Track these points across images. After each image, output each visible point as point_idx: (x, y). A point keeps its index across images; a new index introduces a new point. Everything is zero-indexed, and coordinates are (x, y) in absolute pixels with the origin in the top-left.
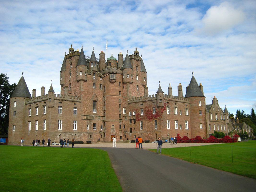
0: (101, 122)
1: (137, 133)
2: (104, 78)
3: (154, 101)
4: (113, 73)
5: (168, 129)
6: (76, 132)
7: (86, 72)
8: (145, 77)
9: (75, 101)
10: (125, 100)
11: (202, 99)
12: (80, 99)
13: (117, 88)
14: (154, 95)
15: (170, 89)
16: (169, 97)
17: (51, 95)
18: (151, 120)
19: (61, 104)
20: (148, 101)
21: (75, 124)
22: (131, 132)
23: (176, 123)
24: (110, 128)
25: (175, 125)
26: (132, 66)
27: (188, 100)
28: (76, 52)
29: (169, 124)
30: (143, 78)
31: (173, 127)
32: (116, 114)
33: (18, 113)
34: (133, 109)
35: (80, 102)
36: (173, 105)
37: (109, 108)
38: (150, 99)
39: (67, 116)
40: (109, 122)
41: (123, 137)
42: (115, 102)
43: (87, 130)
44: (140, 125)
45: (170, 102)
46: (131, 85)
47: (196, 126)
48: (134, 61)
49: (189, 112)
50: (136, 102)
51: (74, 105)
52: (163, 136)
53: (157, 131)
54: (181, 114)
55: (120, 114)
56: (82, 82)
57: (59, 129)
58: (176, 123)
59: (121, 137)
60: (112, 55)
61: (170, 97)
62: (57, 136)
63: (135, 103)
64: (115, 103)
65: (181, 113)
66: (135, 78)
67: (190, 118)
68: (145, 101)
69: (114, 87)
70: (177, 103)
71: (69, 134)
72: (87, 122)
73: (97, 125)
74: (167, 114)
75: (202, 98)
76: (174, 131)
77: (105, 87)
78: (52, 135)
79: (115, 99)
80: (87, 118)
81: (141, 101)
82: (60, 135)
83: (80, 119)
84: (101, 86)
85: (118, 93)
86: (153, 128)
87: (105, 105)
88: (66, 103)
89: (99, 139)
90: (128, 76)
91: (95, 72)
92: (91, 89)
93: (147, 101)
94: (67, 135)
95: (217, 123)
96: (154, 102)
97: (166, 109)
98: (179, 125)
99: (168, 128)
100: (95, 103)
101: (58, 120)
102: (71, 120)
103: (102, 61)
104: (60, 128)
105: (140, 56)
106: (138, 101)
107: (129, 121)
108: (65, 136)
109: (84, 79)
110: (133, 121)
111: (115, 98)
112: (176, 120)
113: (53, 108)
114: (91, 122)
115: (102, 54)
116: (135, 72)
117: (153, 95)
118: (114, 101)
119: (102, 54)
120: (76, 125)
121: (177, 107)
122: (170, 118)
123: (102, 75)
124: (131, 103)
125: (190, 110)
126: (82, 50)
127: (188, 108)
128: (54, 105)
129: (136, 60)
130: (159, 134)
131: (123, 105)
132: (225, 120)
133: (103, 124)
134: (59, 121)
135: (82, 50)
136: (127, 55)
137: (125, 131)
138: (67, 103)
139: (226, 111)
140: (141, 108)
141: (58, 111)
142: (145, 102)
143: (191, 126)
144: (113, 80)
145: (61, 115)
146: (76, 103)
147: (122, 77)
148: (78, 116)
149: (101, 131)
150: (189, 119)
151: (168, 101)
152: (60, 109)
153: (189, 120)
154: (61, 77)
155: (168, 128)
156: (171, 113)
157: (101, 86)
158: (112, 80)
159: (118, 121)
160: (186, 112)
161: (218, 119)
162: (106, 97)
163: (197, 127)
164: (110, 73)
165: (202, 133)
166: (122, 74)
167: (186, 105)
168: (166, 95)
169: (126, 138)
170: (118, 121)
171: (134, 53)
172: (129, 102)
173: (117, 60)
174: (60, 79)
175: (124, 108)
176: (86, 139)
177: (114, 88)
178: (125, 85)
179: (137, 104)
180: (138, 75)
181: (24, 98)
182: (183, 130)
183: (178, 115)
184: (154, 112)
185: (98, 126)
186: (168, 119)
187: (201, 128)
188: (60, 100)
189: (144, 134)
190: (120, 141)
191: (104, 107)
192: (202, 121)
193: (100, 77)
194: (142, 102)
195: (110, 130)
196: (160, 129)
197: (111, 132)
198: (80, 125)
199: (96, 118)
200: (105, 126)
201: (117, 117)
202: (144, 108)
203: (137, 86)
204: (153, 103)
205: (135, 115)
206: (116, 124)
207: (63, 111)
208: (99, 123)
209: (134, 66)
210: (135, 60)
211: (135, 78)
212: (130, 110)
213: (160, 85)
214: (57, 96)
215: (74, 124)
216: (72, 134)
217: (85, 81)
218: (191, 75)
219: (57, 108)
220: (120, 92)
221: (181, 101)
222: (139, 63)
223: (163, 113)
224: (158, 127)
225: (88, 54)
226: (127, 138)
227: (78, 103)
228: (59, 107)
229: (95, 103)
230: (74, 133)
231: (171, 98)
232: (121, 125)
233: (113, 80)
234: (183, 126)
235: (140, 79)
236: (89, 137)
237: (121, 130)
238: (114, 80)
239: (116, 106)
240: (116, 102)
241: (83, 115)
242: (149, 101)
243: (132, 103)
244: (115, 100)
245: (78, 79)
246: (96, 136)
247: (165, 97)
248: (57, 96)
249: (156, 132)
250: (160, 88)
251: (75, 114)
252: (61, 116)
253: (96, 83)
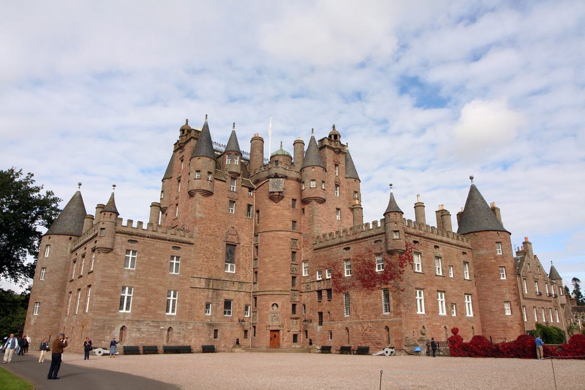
0: (247, 298)
1: (336, 325)
2: (258, 190)
3: (377, 238)
4: (276, 176)
5: (422, 315)
6: (173, 319)
7: (210, 173)
8: (357, 191)
9: (176, 241)
10: (306, 242)
11: (502, 237)
12: (191, 237)
13: (286, 213)
14: (377, 222)
15: (419, 207)
16: (417, 226)
17: (105, 220)
18: (372, 290)
19: (136, 245)
20: (361, 239)
21: (172, 298)
22: (321, 323)
23: (441, 299)
24: (267, 312)
25: (438, 304)
26: (325, 163)
27: (467, 241)
28: (193, 132)
29: (423, 301)
30: (352, 192)
31: (432, 309)
32: (283, 275)
33: (51, 271)
34: (327, 262)
35: (190, 244)
36: (431, 251)
37: (267, 260)
38: (368, 234)
39: (150, 278)
40: (265, 298)
41: (301, 337)
42: (281, 247)
43: (206, 317)
44: (342, 304)
45: (422, 241)
46: (322, 205)
47: (494, 308)
48: (327, 150)
49: (472, 271)
50: (332, 246)
51: (172, 250)
52: (409, 335)
53: (390, 320)
54: (452, 276)
55: (294, 278)
56: (198, 195)
57: (124, 311)
58: (441, 299)
59: (295, 336)
60: (281, 146)
61: (420, 229)
62: (111, 329)
63: (330, 246)
64: (282, 249)
65: (452, 273)
66: (333, 190)
67: (475, 288)
68: (356, 240)
69: (279, 210)
70: (439, 245)
71: (151, 324)
72: (206, 294)
73: (236, 304)
74: (415, 272)
75: (502, 235)
76: (436, 321)
77: (258, 211)
78: (96, 328)
79: (282, 238)
80: (209, 285)
81: (344, 240)
82: (123, 328)
83: (187, 287)
84: (249, 210)
85: (288, 224)
86: (377, 312)
87: (257, 254)
88: (150, 243)
89: (238, 340)
90: (313, 184)
91: (234, 176)
92: (220, 213)
93: (359, 239)
94: (144, 328)
95: (541, 302)
96: (377, 239)
97: (411, 259)
98: (449, 305)
99: (419, 312)
100: (231, 250)
101: (120, 286)
102: (161, 288)
103: (255, 154)
104: (127, 309)
105: (343, 142)
106: (338, 241)
107: (316, 293)
108: (139, 330)
109: (205, 188)
110: (325, 294)
111: (281, 236)
112: (439, 289)
113: (110, 254)
114: (217, 295)
115: (258, 142)
116: (331, 177)
117: (375, 223)
118: (279, 245)
119: (258, 142)
120: (174, 301)
121: (441, 254)
122: (425, 283)
123: (254, 184)
124: (320, 248)
125: (475, 267)
126: (206, 126)
127: (468, 261)
128: (113, 245)
129: (333, 152)
130: (395, 328)
131: (303, 254)
132: (556, 296)
133: (251, 302)
134: (124, 288)
135: (206, 126)
136: (313, 139)
137: (305, 321)
138: (152, 242)
139: (554, 276)
140: (345, 258)
141: (123, 262)
142: (355, 242)
143: (481, 309)
144: (278, 194)
145: (132, 273)
146: (177, 244)
147: (301, 187)
148: (183, 279)
149: (243, 321)
150: (474, 291)
151: (417, 239)
152: (130, 258)
153: (473, 291)
154: (162, 192)
155: (419, 312)
156: (426, 271)
157: (249, 210)
158: (274, 192)
159: (288, 293)
160: (465, 272)
161: (540, 294)
162: (259, 234)
163: (497, 311)
164: (271, 178)
165: (511, 327)
166: (300, 181)
167: (464, 253)
168: (410, 221)
169: (308, 340)
170: (288, 293)
172: (316, 246)
173: (293, 157)
174: (161, 196)
175: (305, 261)
176: (202, 339)
177: (279, 212)
178: (306, 207)
179: (335, 249)
180: (338, 186)
181: (69, 237)
182: (460, 319)
183: (445, 276)
184: (379, 266)
185: (237, 306)
186: (419, 285)
187: (508, 313)
188: (133, 235)
189: (354, 327)
190: (294, 346)
191: (255, 260)
192: (510, 293)
193: (247, 190)
194: (348, 242)
195: (267, 318)
196: (399, 314)
197: (269, 323)
198: (187, 301)
199: (233, 286)
200: (256, 306)
201: (286, 283)
202: (351, 257)
203: (338, 209)
204: (376, 242)
205: (330, 277)
206: (283, 302)
207: (140, 264)
208: (240, 299)
209: (330, 165)
210: (331, 151)
211: (333, 190)
212: (319, 267)
213: (391, 194)
214: (125, 223)
215: (170, 300)
216: (159, 326)
217: (208, 194)
218: (469, 183)
219: (123, 254)
220: (294, 222)
221: (450, 240)
222: (342, 159)
223: (405, 269)
224: (392, 308)
225: (220, 139)
226: (310, 340)
227: (183, 244)
228: (128, 251)
229: (231, 250)
230: (166, 322)
231: (423, 229)
232: (297, 306)
233: (278, 194)
234: (459, 306)
235: (343, 195)
236: (210, 335)
237: (297, 318)
238: (280, 192)
239: (282, 255)
240: (283, 247)
241: (195, 276)
242: (364, 238)
243: (322, 246)
244: (281, 242)
245: (191, 189)
246: (230, 331)
247: (408, 226)
248: (125, 223)
249: (386, 324)
250: (392, 201)
251: (174, 273)
252: (131, 277)
253: (238, 202)
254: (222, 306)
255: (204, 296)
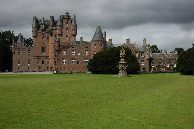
13: (53, 39)
82: (19, 68)
91: (43, 30)
100: (43, 49)
171: (66, 14)
193: (47, 33)
254: (41, 62)
255: (36, 61)
